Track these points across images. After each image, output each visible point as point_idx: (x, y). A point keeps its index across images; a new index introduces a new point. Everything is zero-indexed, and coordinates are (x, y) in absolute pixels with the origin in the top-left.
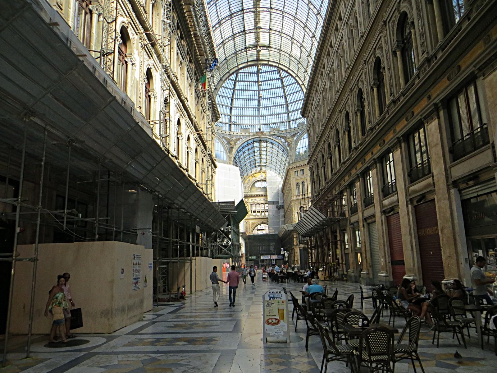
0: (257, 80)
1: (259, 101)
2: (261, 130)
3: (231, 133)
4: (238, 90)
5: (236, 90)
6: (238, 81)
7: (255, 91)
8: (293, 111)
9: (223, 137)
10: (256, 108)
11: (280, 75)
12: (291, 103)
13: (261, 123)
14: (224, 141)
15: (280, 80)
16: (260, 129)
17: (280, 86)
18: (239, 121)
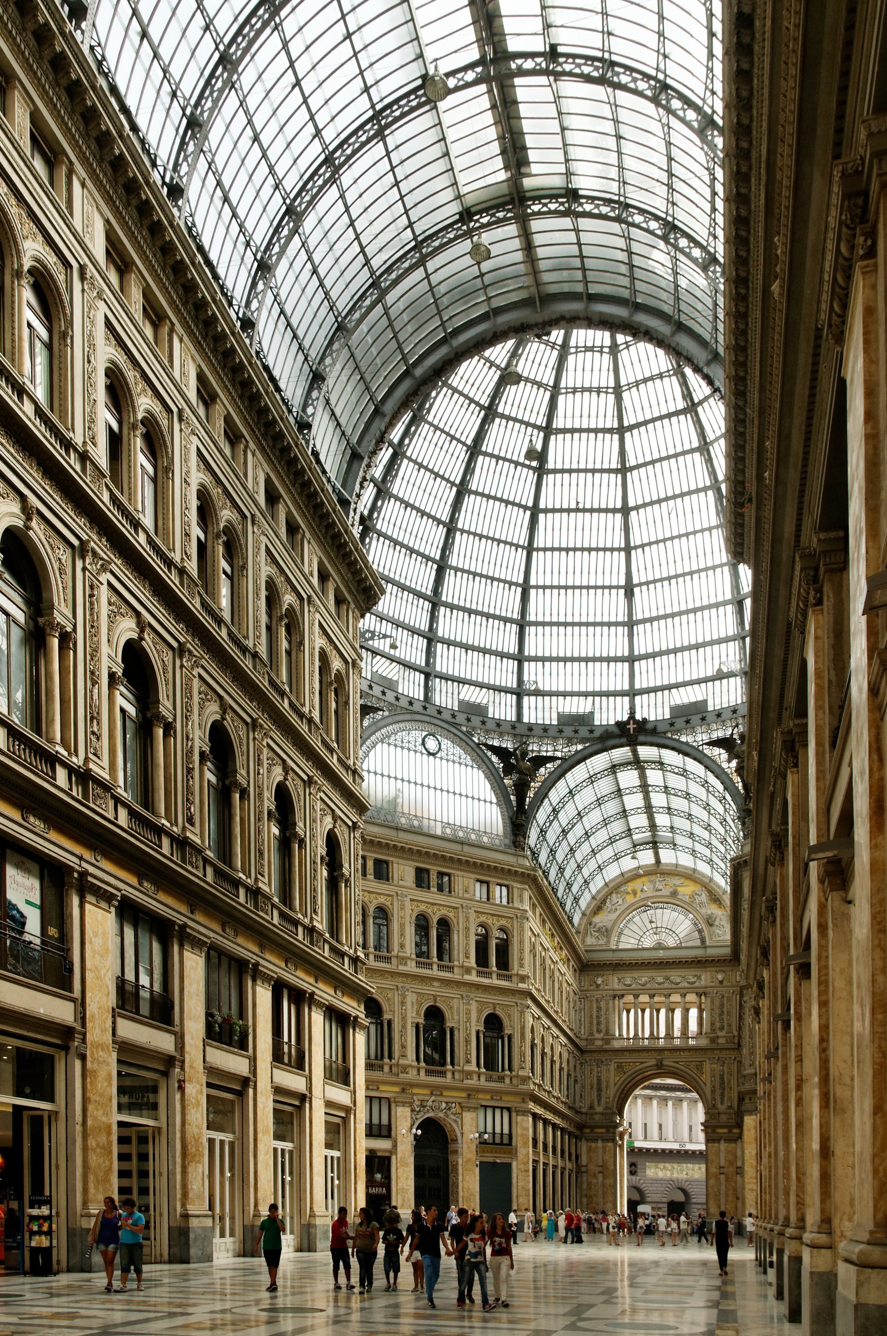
2: (638, 717)
10: (617, 624)
13: (637, 686)
14: (495, 759)
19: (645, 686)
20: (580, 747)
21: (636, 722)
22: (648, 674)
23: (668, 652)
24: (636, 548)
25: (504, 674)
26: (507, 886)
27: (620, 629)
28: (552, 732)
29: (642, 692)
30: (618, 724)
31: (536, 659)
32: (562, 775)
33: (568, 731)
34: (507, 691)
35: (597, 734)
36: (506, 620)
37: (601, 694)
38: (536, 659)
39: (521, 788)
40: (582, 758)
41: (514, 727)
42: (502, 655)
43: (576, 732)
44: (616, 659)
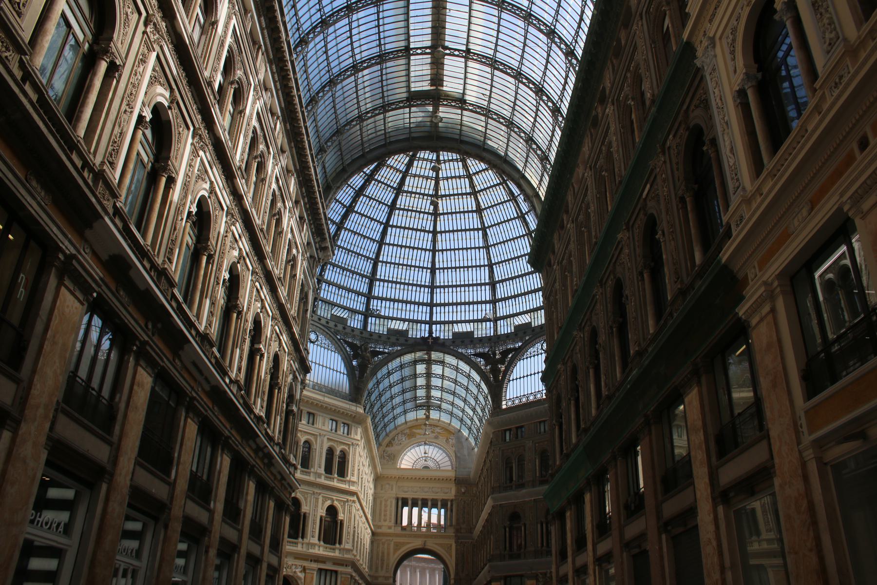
0: (431, 229)
1: (433, 270)
2: (434, 335)
3: (365, 335)
4: (389, 244)
5: (386, 244)
6: (392, 226)
7: (426, 250)
8: (505, 299)
9: (346, 342)
10: (425, 286)
11: (482, 223)
12: (502, 281)
13: (434, 319)
14: (348, 349)
15: (480, 232)
16: (431, 332)
17: (481, 245)
18: (385, 309)
19: (438, 319)
20: (399, 348)
21: (433, 338)
22: (439, 314)
23: (453, 304)
24: (439, 251)
25: (359, 304)
26: (348, 425)
27: (426, 290)
28: (383, 339)
29: (437, 323)
30: (423, 338)
31: (378, 298)
32: (386, 363)
33: (393, 339)
34: (359, 312)
35: (409, 342)
36: (363, 276)
37: (413, 321)
38: (378, 298)
39: (363, 367)
40: (400, 354)
41: (361, 333)
42: (359, 294)
43: (397, 339)
44: (423, 304)
